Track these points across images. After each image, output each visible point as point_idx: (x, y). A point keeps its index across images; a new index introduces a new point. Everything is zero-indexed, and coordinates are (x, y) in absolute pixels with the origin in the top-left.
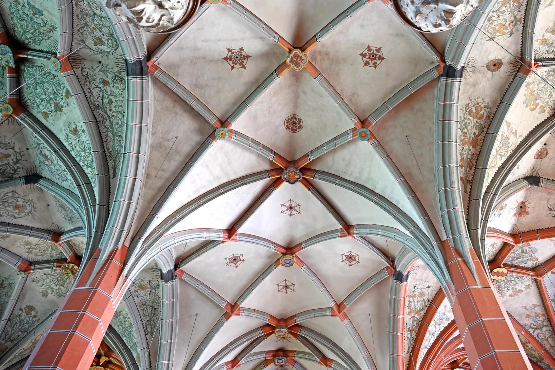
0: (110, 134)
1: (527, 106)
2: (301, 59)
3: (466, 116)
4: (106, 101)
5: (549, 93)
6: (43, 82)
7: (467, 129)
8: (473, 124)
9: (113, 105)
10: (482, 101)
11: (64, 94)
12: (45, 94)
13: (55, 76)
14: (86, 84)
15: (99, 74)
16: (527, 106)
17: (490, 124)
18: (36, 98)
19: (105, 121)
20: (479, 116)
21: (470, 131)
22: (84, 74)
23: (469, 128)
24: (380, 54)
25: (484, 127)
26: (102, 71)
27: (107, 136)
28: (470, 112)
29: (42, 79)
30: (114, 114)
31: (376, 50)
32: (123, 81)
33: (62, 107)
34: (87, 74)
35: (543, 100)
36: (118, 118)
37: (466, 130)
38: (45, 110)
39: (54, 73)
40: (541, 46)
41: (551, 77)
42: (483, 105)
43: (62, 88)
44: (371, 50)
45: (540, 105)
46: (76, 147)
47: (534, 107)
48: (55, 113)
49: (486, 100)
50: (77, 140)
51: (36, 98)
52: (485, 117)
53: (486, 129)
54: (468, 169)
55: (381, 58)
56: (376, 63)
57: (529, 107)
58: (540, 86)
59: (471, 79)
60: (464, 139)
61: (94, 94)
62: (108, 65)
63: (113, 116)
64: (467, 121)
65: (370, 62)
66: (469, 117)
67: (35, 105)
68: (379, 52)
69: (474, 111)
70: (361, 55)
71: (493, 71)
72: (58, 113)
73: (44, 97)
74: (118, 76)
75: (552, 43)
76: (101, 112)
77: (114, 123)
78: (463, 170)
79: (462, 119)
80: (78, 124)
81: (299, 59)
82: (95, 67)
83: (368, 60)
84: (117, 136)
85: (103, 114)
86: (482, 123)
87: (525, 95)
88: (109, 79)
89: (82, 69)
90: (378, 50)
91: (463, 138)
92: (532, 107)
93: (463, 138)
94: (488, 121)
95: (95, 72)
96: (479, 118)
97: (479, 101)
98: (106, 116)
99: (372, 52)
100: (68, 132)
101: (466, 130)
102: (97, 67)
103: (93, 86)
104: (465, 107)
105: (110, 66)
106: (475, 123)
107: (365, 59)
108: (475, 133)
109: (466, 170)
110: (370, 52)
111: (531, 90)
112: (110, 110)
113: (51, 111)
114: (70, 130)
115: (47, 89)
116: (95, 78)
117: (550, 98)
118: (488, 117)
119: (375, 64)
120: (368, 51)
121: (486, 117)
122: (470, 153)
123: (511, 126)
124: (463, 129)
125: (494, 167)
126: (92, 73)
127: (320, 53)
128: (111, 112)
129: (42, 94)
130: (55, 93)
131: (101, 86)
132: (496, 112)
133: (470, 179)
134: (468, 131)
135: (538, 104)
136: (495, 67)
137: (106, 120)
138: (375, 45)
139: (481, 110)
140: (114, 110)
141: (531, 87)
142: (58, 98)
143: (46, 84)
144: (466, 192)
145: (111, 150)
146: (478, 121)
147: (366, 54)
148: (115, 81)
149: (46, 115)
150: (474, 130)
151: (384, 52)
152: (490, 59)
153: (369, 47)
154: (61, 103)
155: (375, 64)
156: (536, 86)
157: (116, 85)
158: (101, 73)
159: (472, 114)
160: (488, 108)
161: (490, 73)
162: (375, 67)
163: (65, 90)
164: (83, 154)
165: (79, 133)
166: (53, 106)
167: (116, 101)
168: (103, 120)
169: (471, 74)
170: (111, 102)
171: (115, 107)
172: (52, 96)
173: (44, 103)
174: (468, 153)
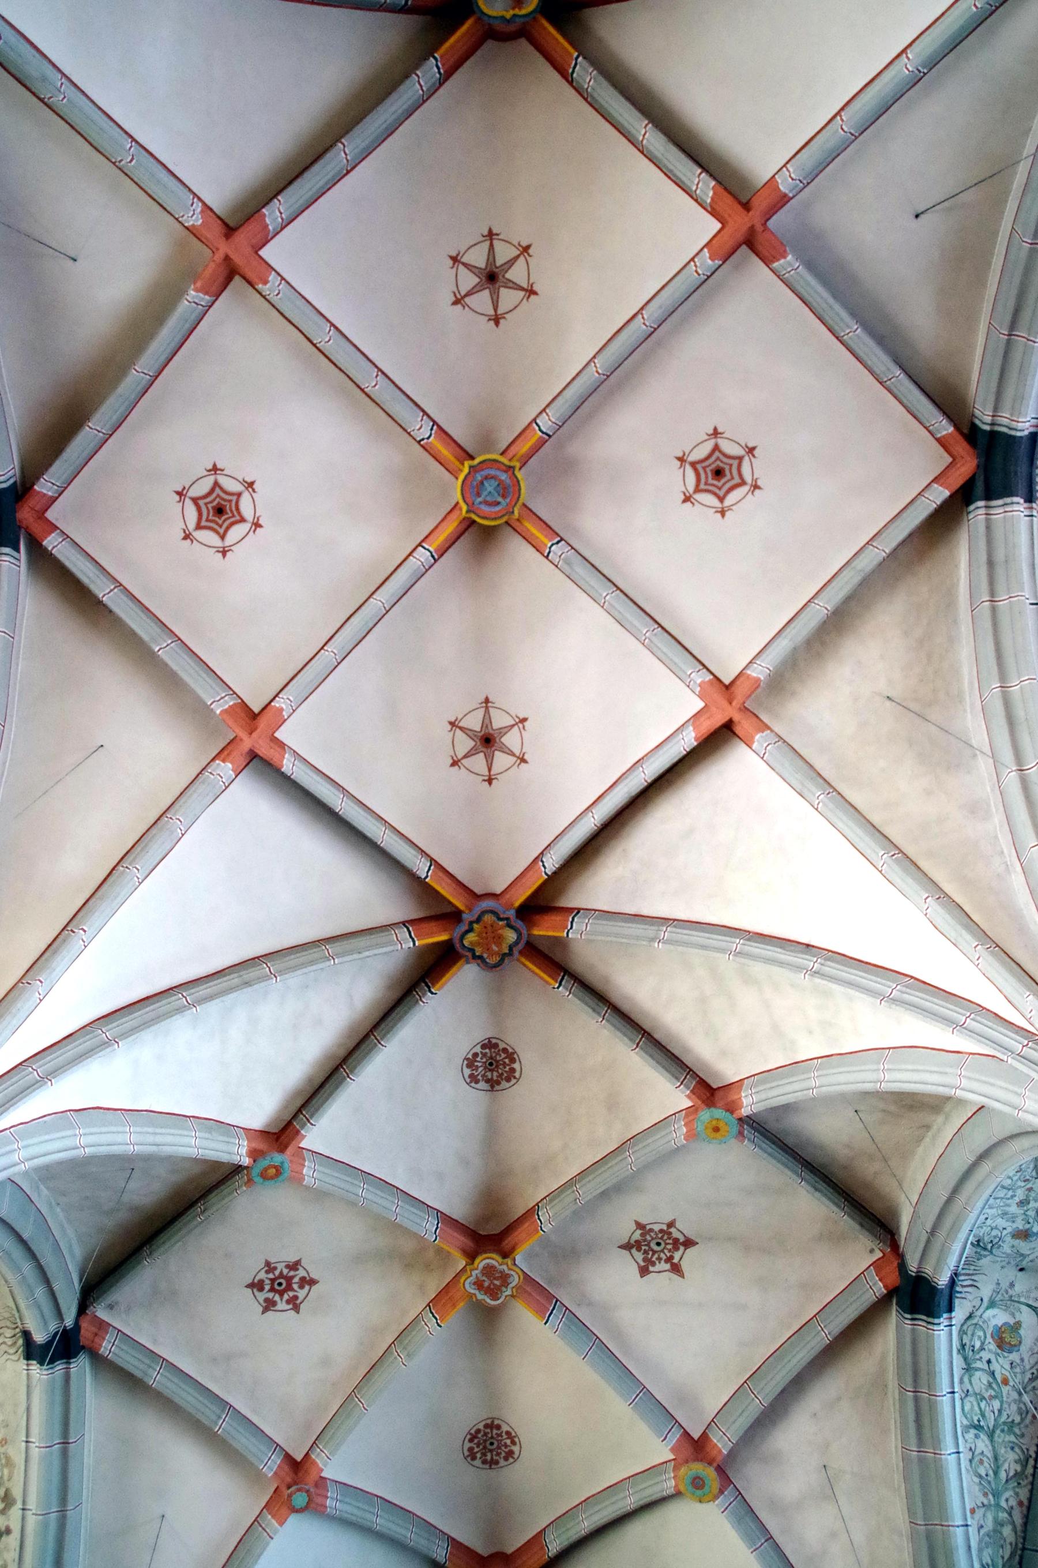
2: (479, 1285)
24: (261, 1296)
31: (274, 1304)
44: (288, 1302)
55: (257, 1286)
56: (267, 1272)
65: (285, 1271)
68: (266, 1300)
70: (312, 1282)
74: (985, 1249)
81: (486, 1284)
83: (292, 1273)
90: (269, 1305)
99: (286, 1297)
107: (301, 1273)
110: (291, 1294)
120: (296, 1297)
127: (428, 1267)
138: (282, 1319)
147: (301, 1287)
151: (251, 1303)
153: (296, 1308)
157: (994, 1233)
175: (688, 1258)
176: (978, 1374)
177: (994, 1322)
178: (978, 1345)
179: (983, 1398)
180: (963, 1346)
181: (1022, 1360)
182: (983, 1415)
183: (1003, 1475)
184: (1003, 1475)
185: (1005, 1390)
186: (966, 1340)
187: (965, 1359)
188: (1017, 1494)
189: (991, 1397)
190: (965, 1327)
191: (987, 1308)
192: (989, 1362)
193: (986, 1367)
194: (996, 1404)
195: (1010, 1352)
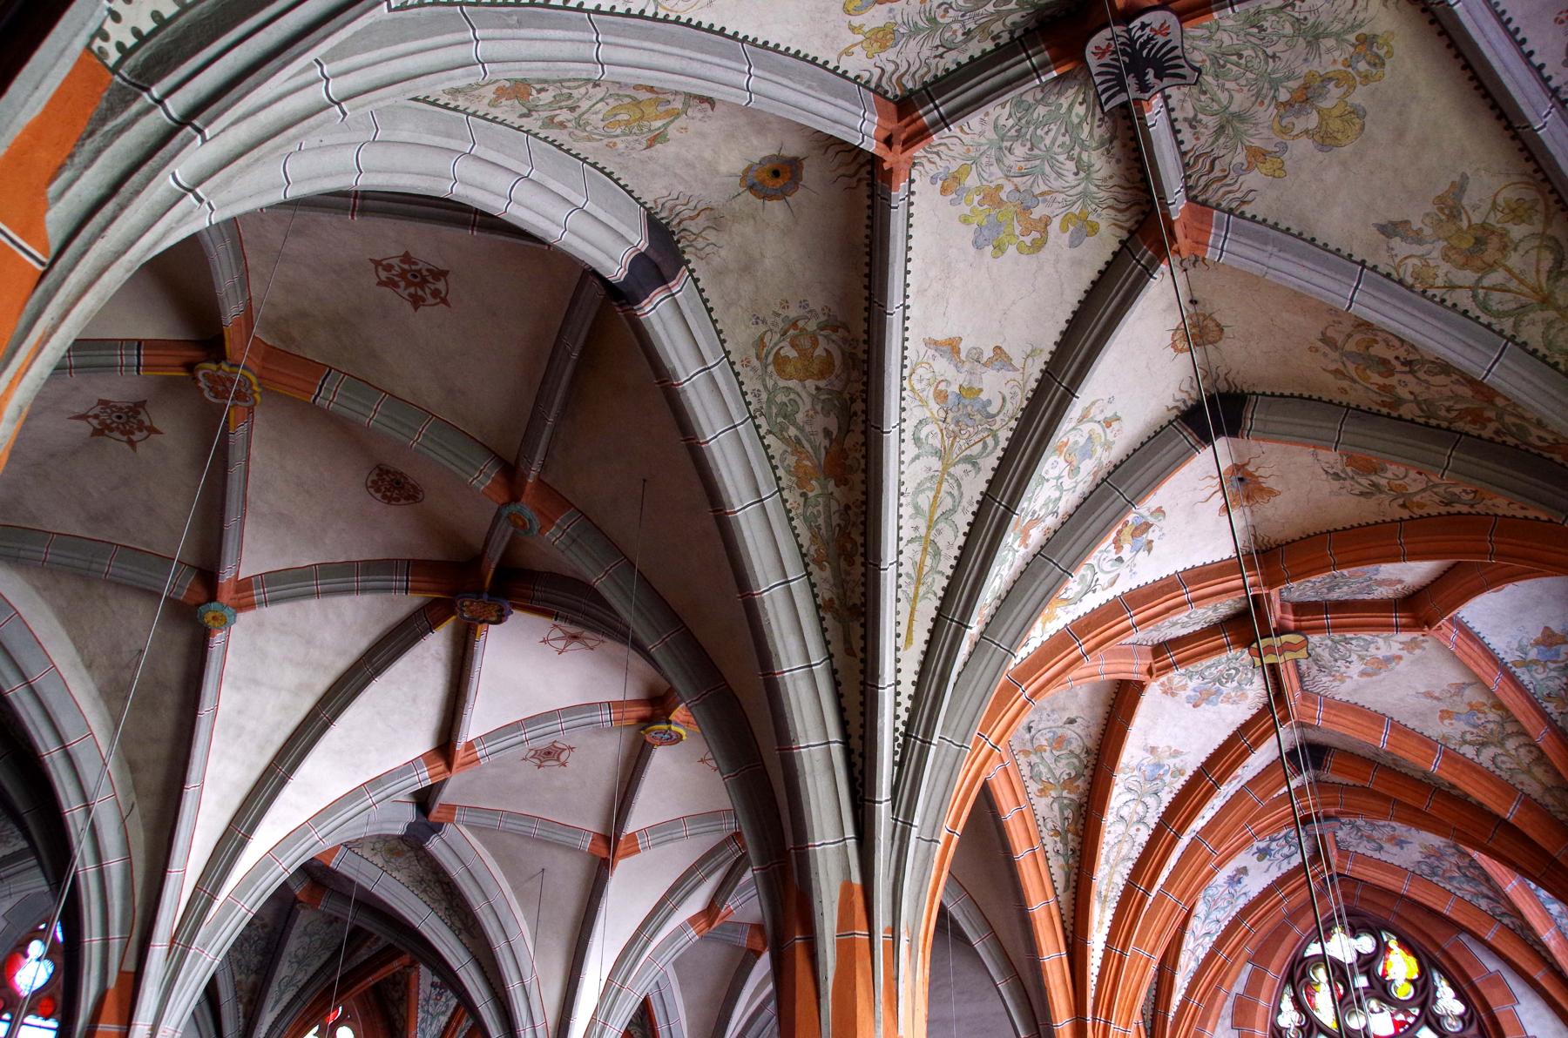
1: (999, 249)
3: (770, 383)
5: (1071, 166)
7: (794, 424)
8: (808, 400)
10: (802, 312)
16: (999, 249)
17: (866, 384)
20: (815, 368)
21: (808, 429)
23: (800, 417)
25: (853, 400)
28: (780, 362)
35: (1060, 197)
37: (792, 431)
40: (891, 54)
41: (1041, 110)
42: (812, 326)
45: (1056, 223)
47: (1035, 235)
49: (817, 303)
52: (838, 362)
53: (858, 406)
54: (843, 564)
57: (1012, 250)
58: (1010, 160)
59: (723, 253)
60: (798, 466)
64: (781, 398)
66: (782, 383)
69: (793, 354)
71: (780, 194)
75: (932, 20)
78: (827, 573)
79: (764, 396)
83: (412, 290)
86: (838, 386)
87: (965, 220)
90: (406, 258)
91: (791, 460)
92: (1028, 240)
93: (791, 460)
94: (855, 374)
96: (822, 375)
97: (793, 313)
101: (792, 431)
104: (752, 352)
106: (814, 398)
108: (827, 433)
109: (836, 572)
111: (978, 190)
117: (1088, 177)
118: (850, 360)
119: (436, 293)
121: (844, 363)
122: (834, 506)
123: (964, 347)
124: (783, 429)
125: (953, 510)
132: (867, 332)
133: (857, 599)
134: (801, 429)
135: (1047, 221)
136: (780, 182)
139: (815, 343)
141: (971, 181)
144: (849, 651)
146: (822, 384)
150: (820, 421)
152: (739, 166)
155: (436, 293)
156: (995, 169)
159: (790, 369)
160: (835, 329)
161: (776, 208)
162: (444, 301)
169: (711, 236)
174: (827, 506)
175: (85, 428)
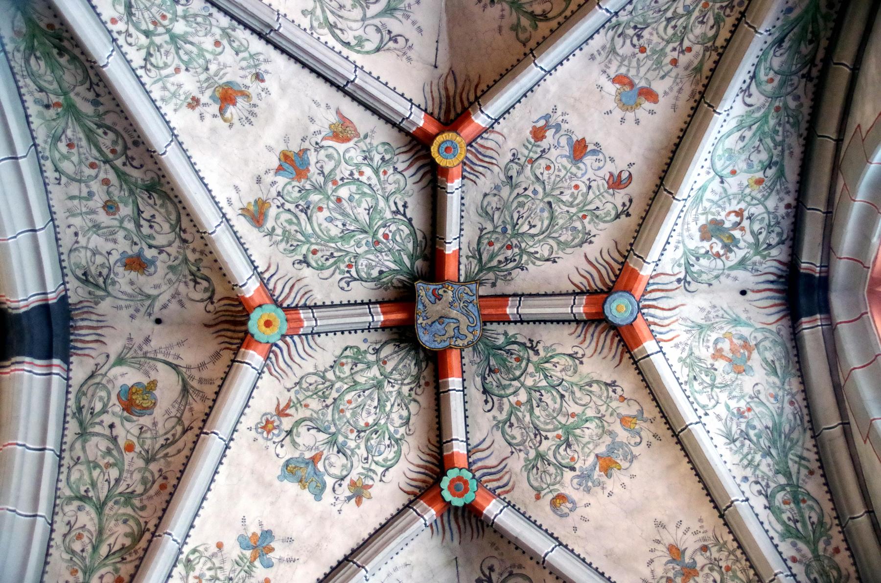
0: (87, 109)
4: (126, 210)
6: (346, 236)
9: (98, 202)
11: (273, 211)
12: (339, 200)
13: (305, 261)
14: (197, 256)
15: (156, 287)
18: (374, 181)
19: (119, 148)
22: (205, 284)
26: (148, 296)
27: (96, 103)
29: (350, 247)
30: (93, 172)
32: (79, 273)
33: (280, 170)
34: (196, 283)
36: (75, 159)
38: (341, 147)
39: (307, 272)
43: (279, 231)
46: (217, 43)
48: (306, 145)
50: (213, 68)
51: (374, 181)
61: (166, 227)
62: (132, 317)
63: (92, 166)
67: (377, 158)
72: (294, 147)
73: (344, 192)
74: (97, 286)
76: (136, 174)
77: (84, 143)
80: (219, 121)
82: (174, 306)
84: (57, 105)
85: (128, 170)
88: (124, 279)
89: (211, 298)
95: (172, 291)
98: (118, 163)
100: (254, 88)
102: (165, 307)
103: (172, 250)
105: (125, 313)
112: (106, 182)
113: (318, 147)
114: (247, 96)
115: (330, 220)
116: (170, 276)
126: (182, 288)
128: (102, 176)
129: (351, 199)
130: (305, 211)
131: (149, 254)
137: (113, 151)
140: (95, 186)
142: (296, 194)
143: (335, 231)
145: (63, 61)
148: (105, 272)
149: (342, 132)
154: (281, 180)
157: (99, 260)
158: (154, 292)
163: (269, 224)
164: (180, 27)
165: (209, 93)
166: (313, 169)
167: (93, 212)
168: (126, 148)
170: (110, 207)
171: (91, 194)
172: (315, 198)
173: (344, 170)
176: (94, 440)
177: (121, 382)
178: (98, 406)
179: (96, 466)
180: (80, 409)
181: (155, 424)
182: (94, 484)
183: (104, 550)
184: (104, 550)
185: (128, 456)
186: (84, 401)
187: (81, 423)
188: (117, 570)
189: (108, 465)
190: (84, 388)
191: (114, 365)
192: (112, 426)
193: (107, 432)
194: (114, 473)
195: (141, 415)
